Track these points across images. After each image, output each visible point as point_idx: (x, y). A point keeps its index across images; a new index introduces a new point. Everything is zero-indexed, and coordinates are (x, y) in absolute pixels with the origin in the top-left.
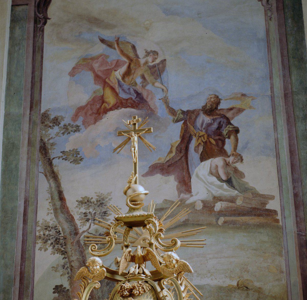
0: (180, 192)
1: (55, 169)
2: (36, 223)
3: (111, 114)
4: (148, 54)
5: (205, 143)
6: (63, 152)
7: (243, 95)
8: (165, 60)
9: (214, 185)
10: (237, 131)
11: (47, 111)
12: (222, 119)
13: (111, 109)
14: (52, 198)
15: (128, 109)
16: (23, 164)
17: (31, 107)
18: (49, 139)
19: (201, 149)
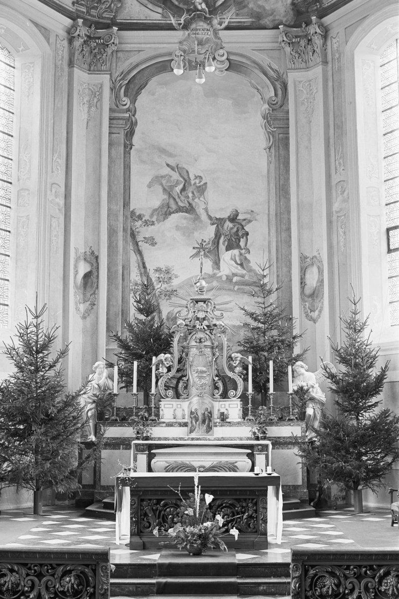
0: (214, 269)
1: (140, 248)
2: (130, 281)
3: (173, 215)
4: (196, 177)
5: (229, 240)
6: (144, 238)
7: (252, 211)
8: (206, 183)
9: (234, 267)
10: (247, 234)
11: (134, 209)
12: (239, 226)
13: (173, 213)
14: (139, 267)
15: (184, 214)
16: (121, 243)
17: (124, 206)
18: (135, 229)
19: (226, 243)
